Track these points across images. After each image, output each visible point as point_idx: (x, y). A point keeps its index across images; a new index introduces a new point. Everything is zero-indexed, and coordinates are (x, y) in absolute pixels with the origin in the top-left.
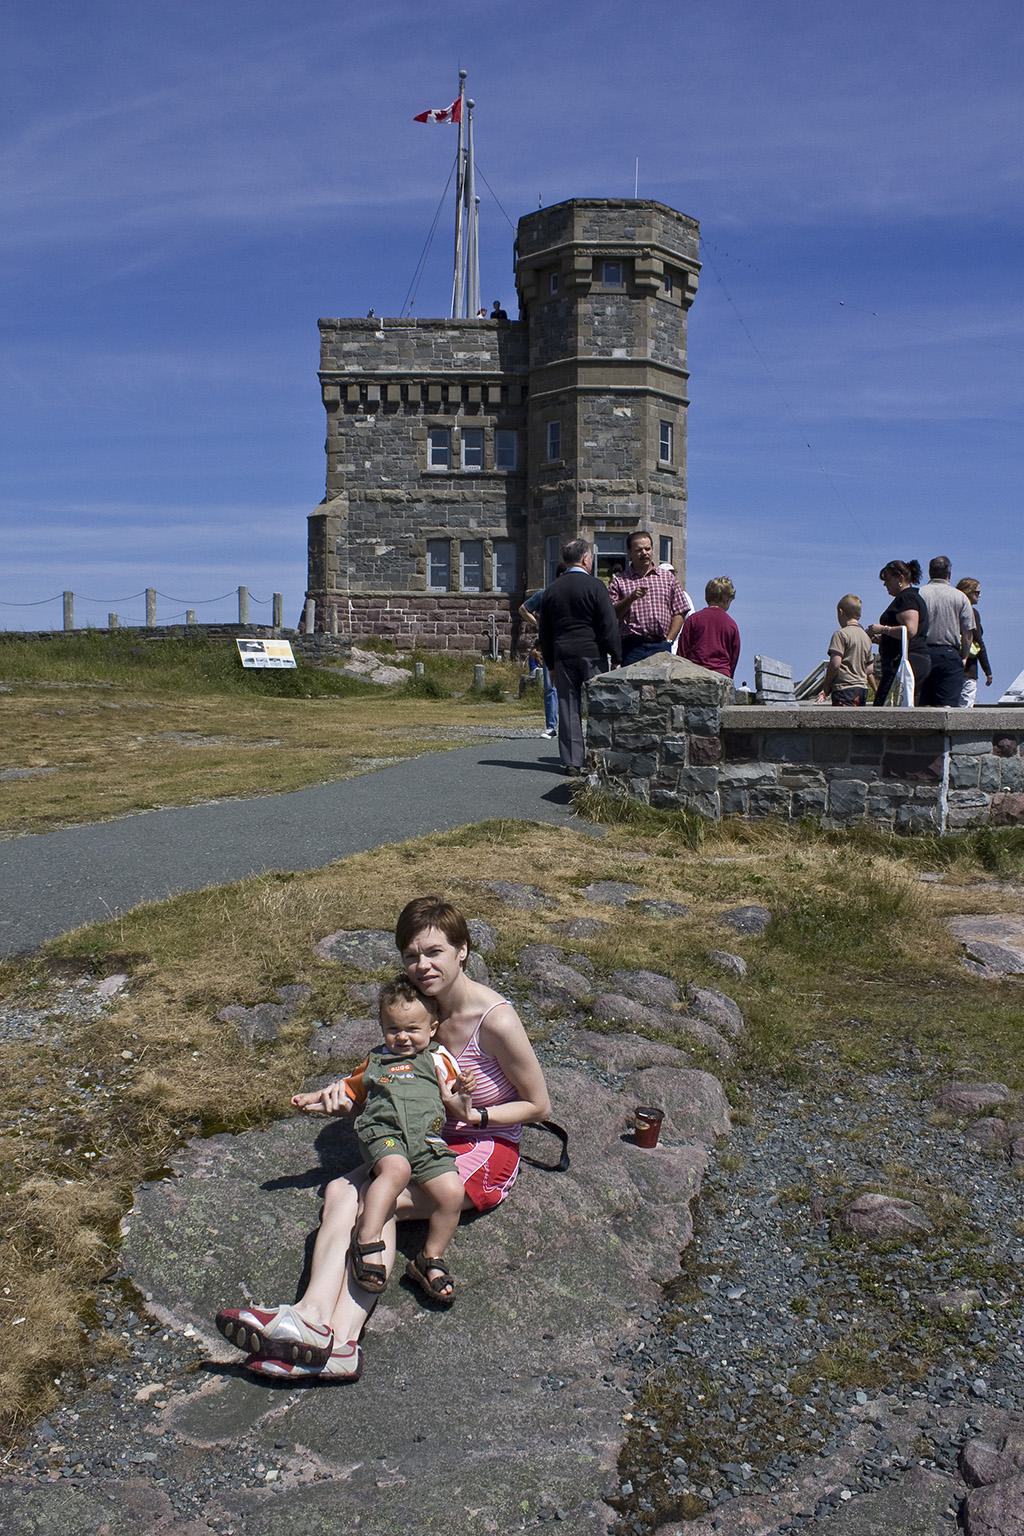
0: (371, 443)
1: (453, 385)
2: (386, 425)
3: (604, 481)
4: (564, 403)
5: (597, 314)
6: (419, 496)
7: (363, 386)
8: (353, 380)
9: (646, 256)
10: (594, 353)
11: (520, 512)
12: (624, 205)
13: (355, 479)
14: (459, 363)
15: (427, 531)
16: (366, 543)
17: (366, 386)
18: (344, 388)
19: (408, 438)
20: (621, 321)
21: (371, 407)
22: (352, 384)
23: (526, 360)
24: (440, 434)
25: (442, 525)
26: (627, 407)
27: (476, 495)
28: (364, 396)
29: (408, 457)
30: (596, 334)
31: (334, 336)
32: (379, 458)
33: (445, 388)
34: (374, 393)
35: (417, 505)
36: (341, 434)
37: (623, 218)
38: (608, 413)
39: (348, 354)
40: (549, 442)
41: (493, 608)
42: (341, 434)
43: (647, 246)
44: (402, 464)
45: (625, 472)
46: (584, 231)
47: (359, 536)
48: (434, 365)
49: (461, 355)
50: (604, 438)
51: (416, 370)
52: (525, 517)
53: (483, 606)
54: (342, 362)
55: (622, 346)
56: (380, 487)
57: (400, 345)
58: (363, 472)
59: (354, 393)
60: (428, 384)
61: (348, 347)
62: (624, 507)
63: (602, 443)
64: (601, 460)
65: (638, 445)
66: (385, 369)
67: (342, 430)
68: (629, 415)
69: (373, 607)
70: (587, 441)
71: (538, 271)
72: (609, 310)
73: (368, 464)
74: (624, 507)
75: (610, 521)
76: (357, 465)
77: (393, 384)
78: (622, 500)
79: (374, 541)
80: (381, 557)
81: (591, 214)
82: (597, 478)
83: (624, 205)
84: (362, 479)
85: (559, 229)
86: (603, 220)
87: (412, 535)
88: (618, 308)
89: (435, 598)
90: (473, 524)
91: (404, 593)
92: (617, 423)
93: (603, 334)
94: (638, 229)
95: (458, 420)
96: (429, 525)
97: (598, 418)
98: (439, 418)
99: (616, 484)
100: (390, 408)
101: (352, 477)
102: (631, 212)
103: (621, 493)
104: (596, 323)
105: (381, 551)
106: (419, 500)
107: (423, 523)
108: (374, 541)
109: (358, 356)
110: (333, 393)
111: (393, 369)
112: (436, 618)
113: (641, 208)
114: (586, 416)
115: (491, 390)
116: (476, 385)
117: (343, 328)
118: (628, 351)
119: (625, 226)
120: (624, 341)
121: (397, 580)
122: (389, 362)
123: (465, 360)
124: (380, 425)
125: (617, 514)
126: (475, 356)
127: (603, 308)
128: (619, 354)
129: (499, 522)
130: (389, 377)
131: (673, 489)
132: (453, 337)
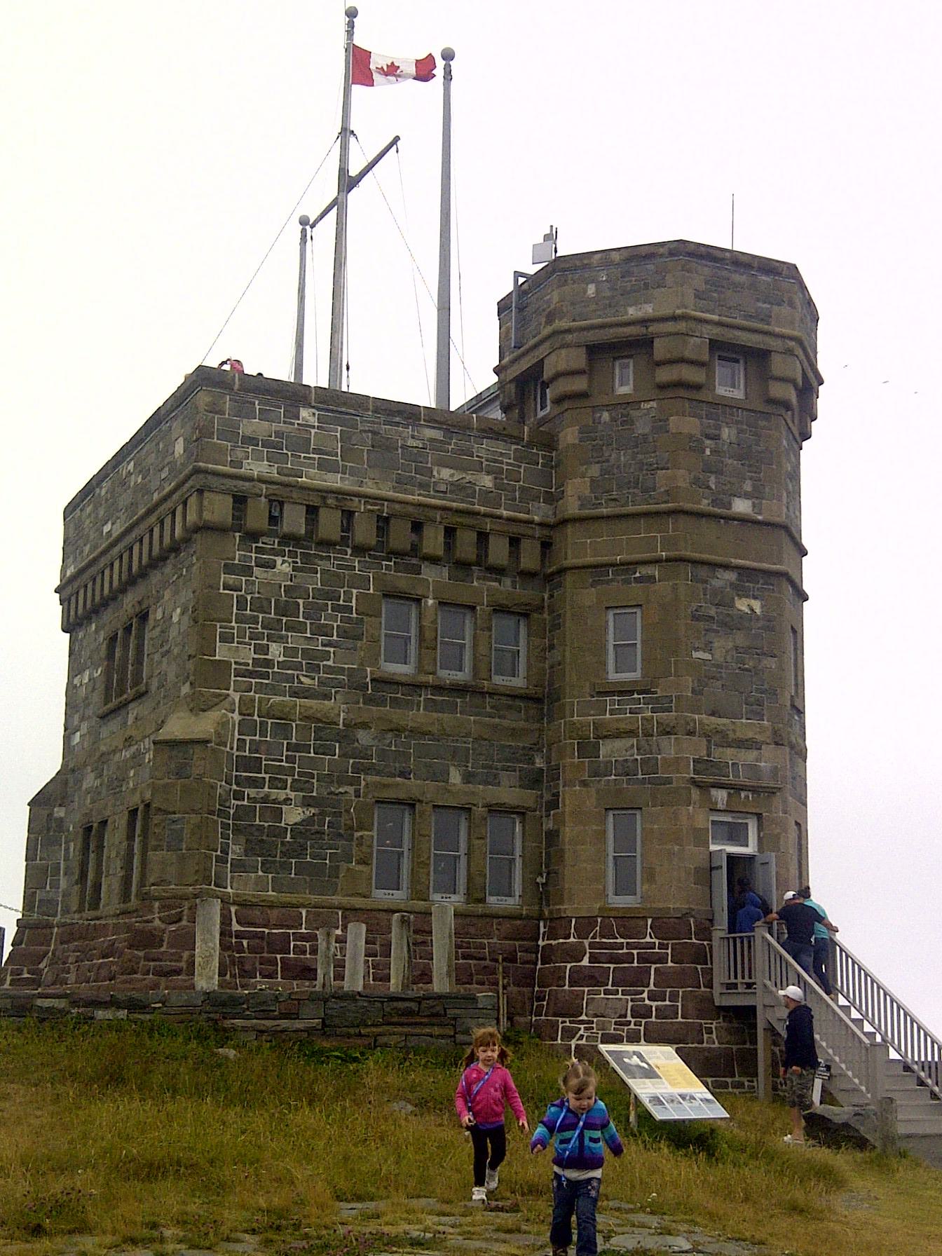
0: (286, 609)
3: (724, 721)
4: (651, 579)
5: (708, 437)
6: (365, 717)
7: (276, 503)
9: (789, 352)
10: (706, 501)
11: (533, 763)
12: (756, 265)
13: (251, 674)
14: (443, 488)
16: (265, 799)
17: (281, 504)
18: (240, 501)
20: (744, 454)
25: (404, 774)
26: (755, 598)
30: (708, 469)
32: (294, 640)
33: (417, 527)
34: (294, 520)
41: (489, 936)
43: (791, 338)
46: (696, 296)
47: (257, 783)
48: (400, 483)
49: (446, 473)
50: (723, 646)
51: (369, 489)
52: (541, 770)
53: (472, 930)
54: (239, 454)
55: (747, 496)
56: (295, 694)
57: (345, 438)
58: (268, 663)
59: (257, 516)
61: (253, 426)
62: (753, 768)
63: (719, 656)
64: (719, 683)
65: (771, 663)
66: (312, 477)
67: (231, 579)
68: (758, 611)
69: (276, 926)
70: (697, 649)
71: (595, 351)
72: (726, 433)
74: (753, 768)
75: (735, 789)
77: (327, 506)
79: (282, 794)
80: (300, 830)
82: (713, 714)
83: (756, 265)
84: (266, 676)
85: (646, 286)
86: (725, 283)
87: (351, 789)
88: (740, 431)
90: (455, 777)
91: (336, 899)
93: (719, 472)
94: (776, 308)
97: (713, 612)
99: (744, 727)
104: (708, 452)
105: (294, 815)
106: (365, 726)
107: (368, 770)
108: (282, 794)
109: (273, 447)
111: (335, 481)
113: (780, 274)
114: (694, 605)
116: (471, 527)
118: (754, 506)
119: (758, 300)
120: (748, 486)
121: (323, 877)
122: (323, 466)
123: (452, 484)
125: (742, 779)
126: (469, 478)
127: (719, 428)
128: (741, 506)
129: (496, 776)
130: (324, 493)
132: (432, 440)
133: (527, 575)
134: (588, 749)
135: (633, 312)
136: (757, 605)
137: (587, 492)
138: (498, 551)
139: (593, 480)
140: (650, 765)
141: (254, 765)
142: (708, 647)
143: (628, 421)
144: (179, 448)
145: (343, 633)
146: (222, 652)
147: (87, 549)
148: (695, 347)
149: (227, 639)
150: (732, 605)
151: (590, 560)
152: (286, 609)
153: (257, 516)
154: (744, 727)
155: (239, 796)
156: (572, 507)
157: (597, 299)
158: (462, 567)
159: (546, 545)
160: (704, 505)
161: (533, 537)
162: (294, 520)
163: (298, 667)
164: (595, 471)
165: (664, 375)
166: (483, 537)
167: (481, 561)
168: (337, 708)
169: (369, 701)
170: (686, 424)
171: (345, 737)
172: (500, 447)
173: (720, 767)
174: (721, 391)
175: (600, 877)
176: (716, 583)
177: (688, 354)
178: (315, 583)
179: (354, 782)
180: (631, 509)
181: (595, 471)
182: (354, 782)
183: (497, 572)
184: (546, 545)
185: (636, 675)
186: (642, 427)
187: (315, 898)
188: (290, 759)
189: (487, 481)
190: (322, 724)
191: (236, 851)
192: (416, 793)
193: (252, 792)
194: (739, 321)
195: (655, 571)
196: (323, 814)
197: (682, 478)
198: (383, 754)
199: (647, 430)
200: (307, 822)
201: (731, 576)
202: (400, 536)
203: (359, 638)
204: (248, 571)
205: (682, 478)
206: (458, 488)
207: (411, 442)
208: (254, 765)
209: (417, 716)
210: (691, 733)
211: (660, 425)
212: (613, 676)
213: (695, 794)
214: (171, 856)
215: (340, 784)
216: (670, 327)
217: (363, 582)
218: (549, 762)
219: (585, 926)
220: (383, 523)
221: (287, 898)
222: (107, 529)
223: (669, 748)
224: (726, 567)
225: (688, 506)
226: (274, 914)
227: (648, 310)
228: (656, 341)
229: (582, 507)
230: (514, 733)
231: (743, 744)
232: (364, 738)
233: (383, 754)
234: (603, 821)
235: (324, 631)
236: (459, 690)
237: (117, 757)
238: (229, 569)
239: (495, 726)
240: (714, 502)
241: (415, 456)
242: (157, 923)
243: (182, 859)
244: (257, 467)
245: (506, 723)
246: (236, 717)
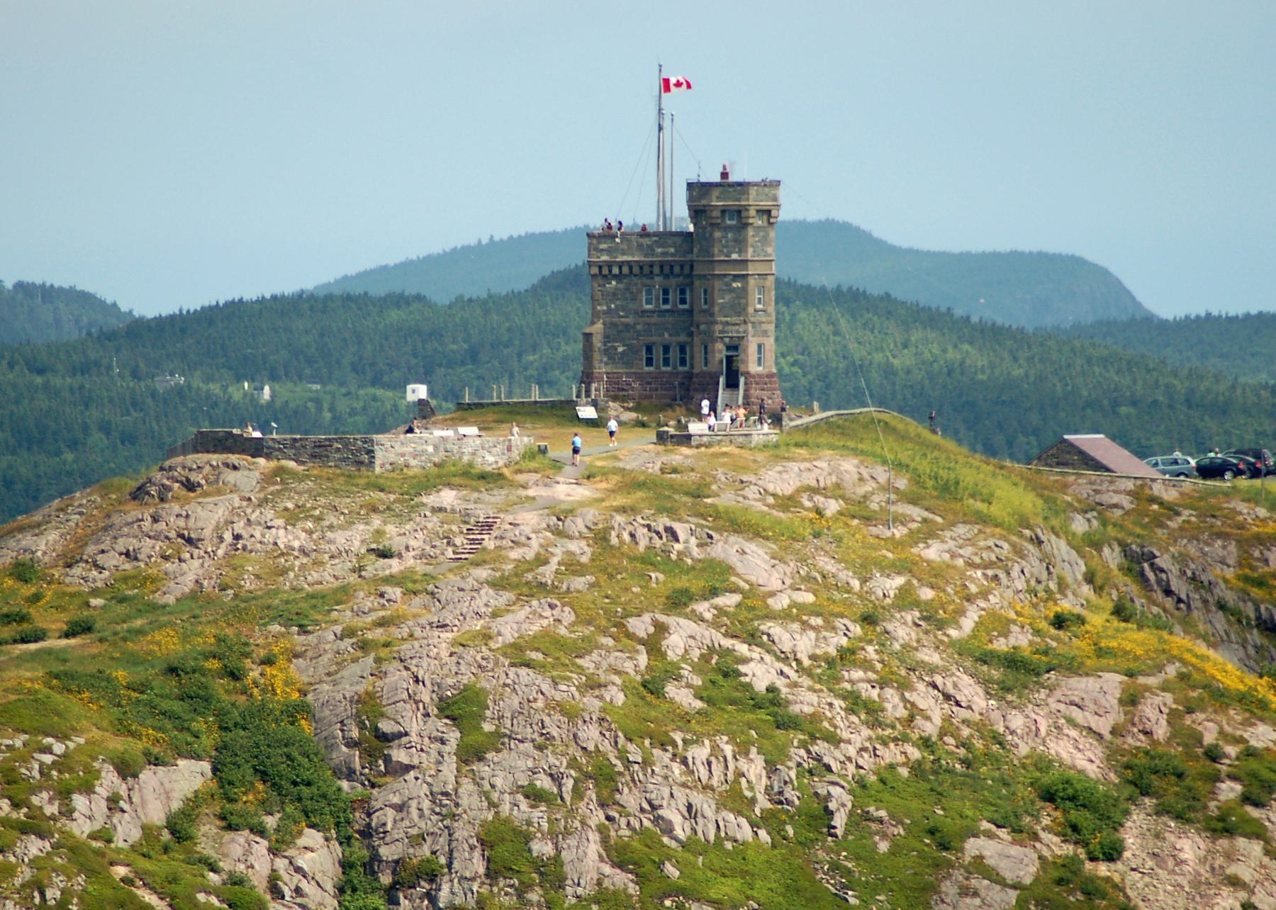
2: (621, 286)
18: (600, 268)
20: (735, 240)
21: (615, 277)
28: (610, 271)
31: (595, 241)
32: (618, 303)
34: (616, 270)
38: (729, 285)
44: (631, 306)
45: (739, 314)
48: (646, 256)
50: (728, 297)
59: (605, 271)
62: (738, 332)
66: (620, 259)
72: (730, 235)
75: (731, 338)
80: (623, 353)
81: (720, 189)
90: (666, 335)
92: (734, 290)
99: (734, 319)
101: (605, 313)
105: (620, 349)
109: (608, 251)
110: (595, 270)
112: (649, 383)
122: (623, 254)
128: (735, 256)
131: (764, 319)
134: (698, 327)
138: (677, 270)
152: (614, 294)
153: (605, 271)
154: (734, 319)
159: (692, 267)
162: (616, 270)
166: (672, 267)
167: (672, 273)
168: (630, 320)
174: (728, 222)
183: (678, 276)
189: (672, 250)
190: (627, 326)
202: (647, 270)
206: (664, 254)
209: (655, 319)
219: (698, 375)
220: (641, 268)
232: (639, 327)
236: (667, 311)
244: (605, 258)
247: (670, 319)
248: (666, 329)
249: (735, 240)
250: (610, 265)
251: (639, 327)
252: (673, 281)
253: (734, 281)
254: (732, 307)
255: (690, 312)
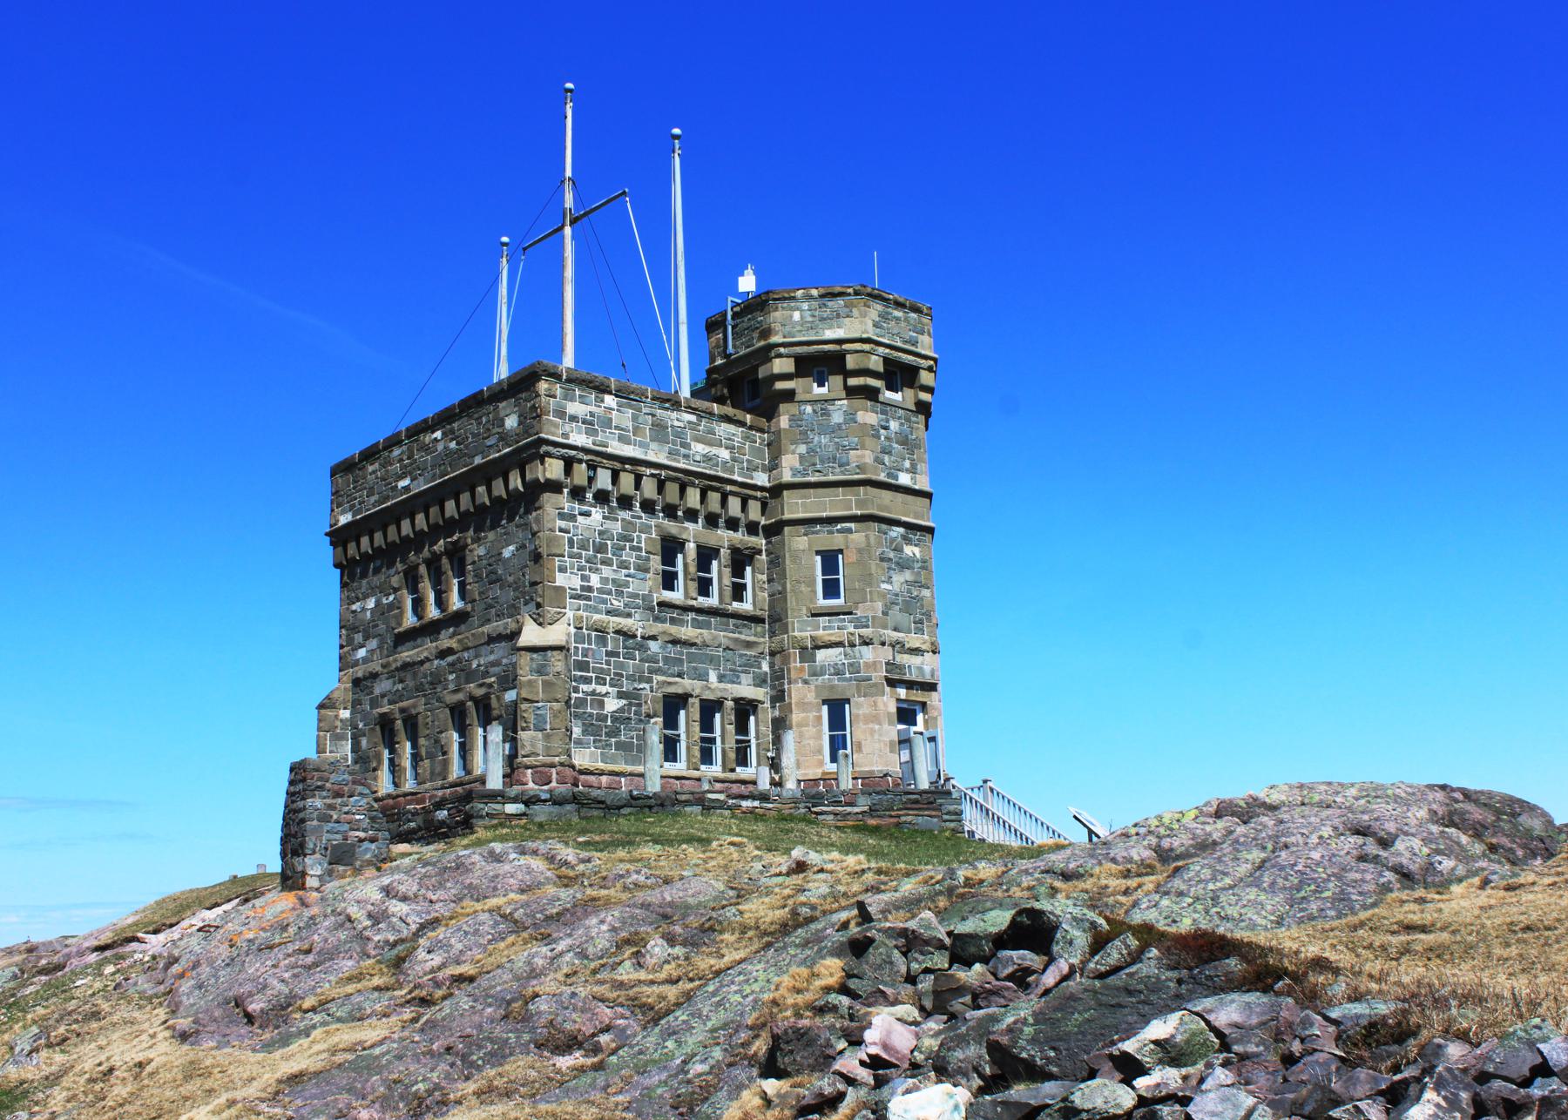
0: (601, 548)
1: (693, 485)
4: (849, 531)
7: (592, 467)
8: (581, 455)
15: (664, 682)
16: (593, 693)
18: (569, 464)
19: (640, 549)
21: (602, 497)
22: (580, 461)
23: (773, 466)
24: (670, 548)
25: (680, 675)
27: (715, 638)
29: (641, 575)
30: (884, 451)
32: (607, 572)
35: (651, 644)
36: (561, 530)
37: (906, 320)
38: (898, 549)
39: (573, 418)
40: (819, 578)
42: (561, 530)
47: (587, 681)
49: (699, 448)
50: (900, 579)
51: (651, 457)
55: (907, 471)
56: (608, 613)
57: (635, 418)
58: (590, 589)
59: (581, 473)
60: (669, 479)
61: (574, 408)
62: (920, 669)
65: (926, 593)
66: (616, 448)
67: (563, 524)
72: (894, 425)
73: (595, 581)
75: (910, 685)
76: (584, 578)
78: (915, 660)
79: (602, 689)
81: (878, 307)
82: (895, 630)
84: (589, 598)
85: (838, 316)
87: (647, 686)
89: (677, 778)
90: (713, 676)
93: (889, 453)
95: (692, 532)
96: (664, 674)
97: (892, 555)
98: (672, 527)
99: (914, 640)
100: (625, 502)
102: (913, 315)
103: (916, 651)
105: (612, 705)
106: (654, 638)
107: (658, 671)
108: (602, 689)
109: (589, 424)
115: (730, 498)
116: (716, 490)
117: (569, 381)
120: (907, 464)
122: (623, 439)
124: (609, 525)
125: (914, 678)
128: (904, 479)
133: (752, 528)
135: (829, 334)
136: (917, 550)
137: (797, 465)
139: (801, 456)
140: (855, 668)
141: (583, 666)
142: (889, 581)
143: (826, 413)
144: (511, 422)
145: (638, 568)
146: (560, 580)
147: (373, 499)
148: (876, 363)
149: (562, 570)
150: (901, 551)
151: (801, 515)
152: (601, 548)
155: (576, 690)
156: (787, 477)
157: (803, 321)
158: (712, 521)
160: (882, 477)
161: (755, 498)
163: (610, 593)
164: (802, 449)
165: (852, 382)
168: (636, 624)
169: (656, 619)
170: (868, 416)
171: (642, 648)
172: (732, 428)
173: (901, 667)
175: (820, 751)
176: (893, 534)
177: (872, 366)
178: (617, 528)
179: (649, 681)
180: (831, 478)
181: (802, 449)
182: (649, 681)
183: (732, 524)
184: (764, 506)
185: (840, 602)
186: (837, 418)
187: (629, 768)
188: (608, 663)
189: (725, 454)
191: (577, 731)
192: (689, 690)
193: (584, 687)
194: (899, 344)
195: (852, 525)
196: (630, 704)
197: (868, 457)
198: (666, 659)
199: (841, 420)
200: (621, 710)
201: (901, 530)
203: (647, 570)
204: (572, 518)
205: (868, 457)
206: (707, 458)
207: (676, 423)
208: (583, 666)
210: (883, 644)
211: (850, 416)
212: (822, 602)
213: (888, 689)
214: (540, 734)
215: (641, 680)
216: (857, 346)
217: (646, 529)
218: (772, 665)
221: (610, 767)
222: (402, 484)
223: (868, 654)
224: (898, 523)
225: (874, 477)
226: (604, 779)
227: (839, 333)
228: (848, 357)
229: (794, 475)
230: (749, 645)
231: (916, 651)
233: (666, 659)
234: (820, 710)
235: (624, 565)
237: (427, 665)
238: (562, 516)
239: (736, 640)
240: (889, 475)
241: (679, 434)
242: (531, 785)
243: (547, 737)
244: (579, 439)
245: (743, 637)
246: (572, 630)
247: (715, 634)
248: (714, 661)
249: (904, 441)
250: (596, 459)
251: (654, 646)
252: (724, 537)
253: (908, 541)
254: (907, 608)
255: (776, 619)
